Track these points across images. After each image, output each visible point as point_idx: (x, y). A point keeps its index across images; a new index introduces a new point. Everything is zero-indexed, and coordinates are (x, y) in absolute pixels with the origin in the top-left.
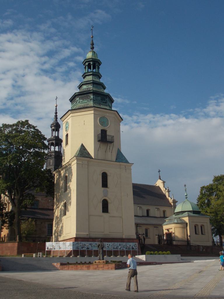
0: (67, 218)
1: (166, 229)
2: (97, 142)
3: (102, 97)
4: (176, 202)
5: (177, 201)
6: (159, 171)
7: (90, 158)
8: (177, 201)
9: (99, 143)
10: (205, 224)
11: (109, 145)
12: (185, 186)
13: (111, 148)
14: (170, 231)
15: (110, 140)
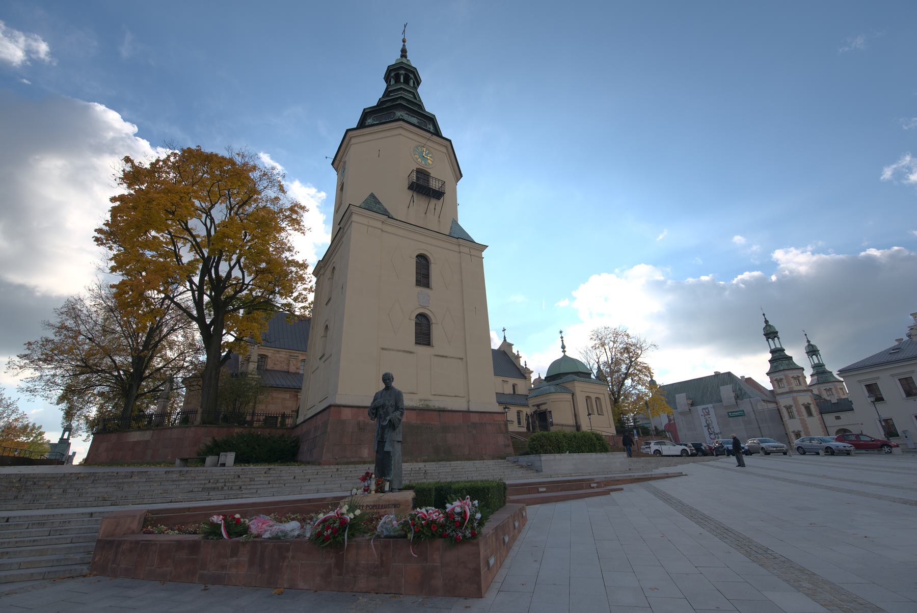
0: (325, 361)
1: (533, 406)
2: (407, 190)
3: (421, 120)
4: (531, 373)
5: (532, 372)
6: (504, 330)
7: (389, 217)
8: (532, 372)
9: (410, 193)
10: (601, 396)
11: (433, 202)
12: (561, 332)
13: (438, 208)
14: (543, 408)
15: (437, 187)
